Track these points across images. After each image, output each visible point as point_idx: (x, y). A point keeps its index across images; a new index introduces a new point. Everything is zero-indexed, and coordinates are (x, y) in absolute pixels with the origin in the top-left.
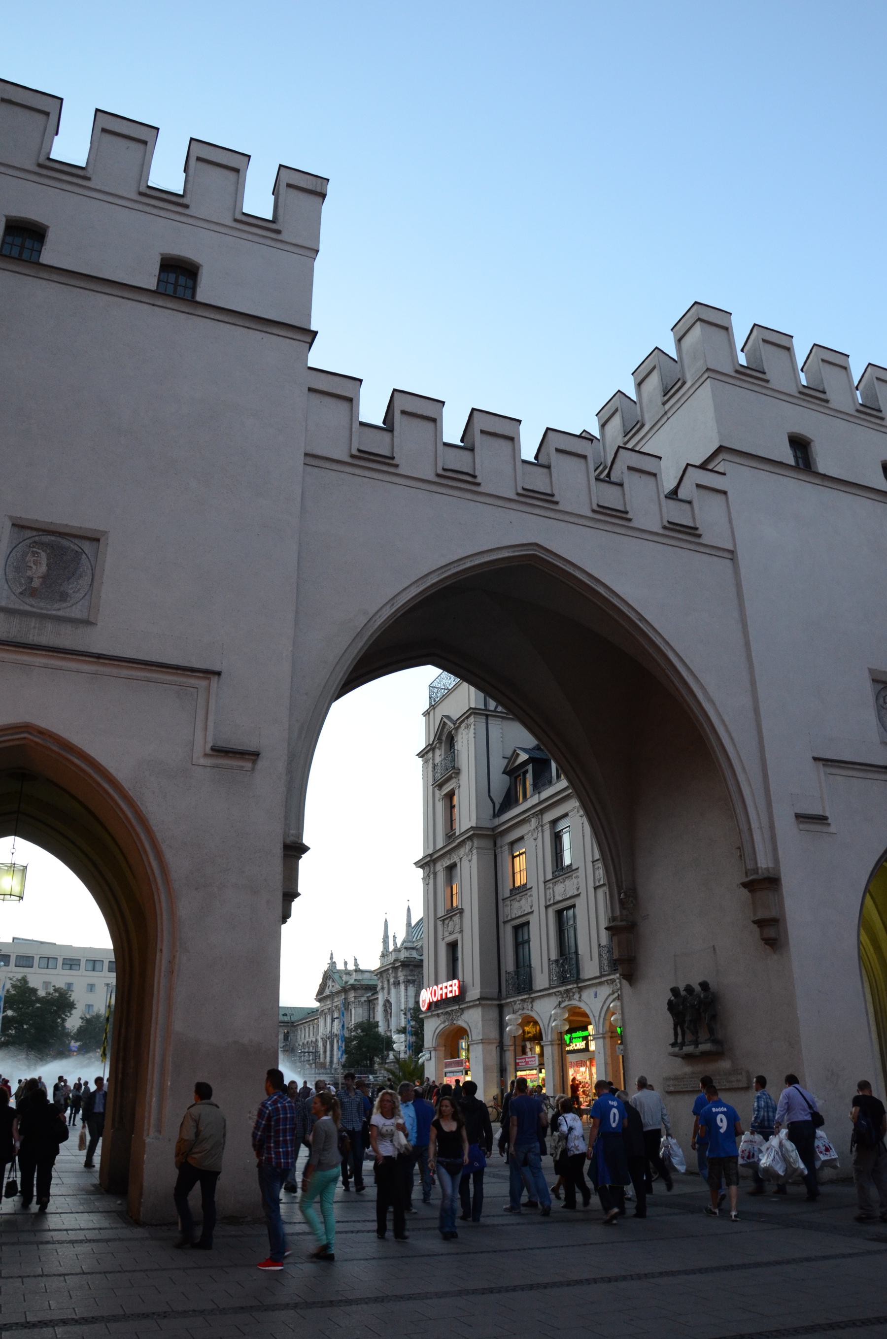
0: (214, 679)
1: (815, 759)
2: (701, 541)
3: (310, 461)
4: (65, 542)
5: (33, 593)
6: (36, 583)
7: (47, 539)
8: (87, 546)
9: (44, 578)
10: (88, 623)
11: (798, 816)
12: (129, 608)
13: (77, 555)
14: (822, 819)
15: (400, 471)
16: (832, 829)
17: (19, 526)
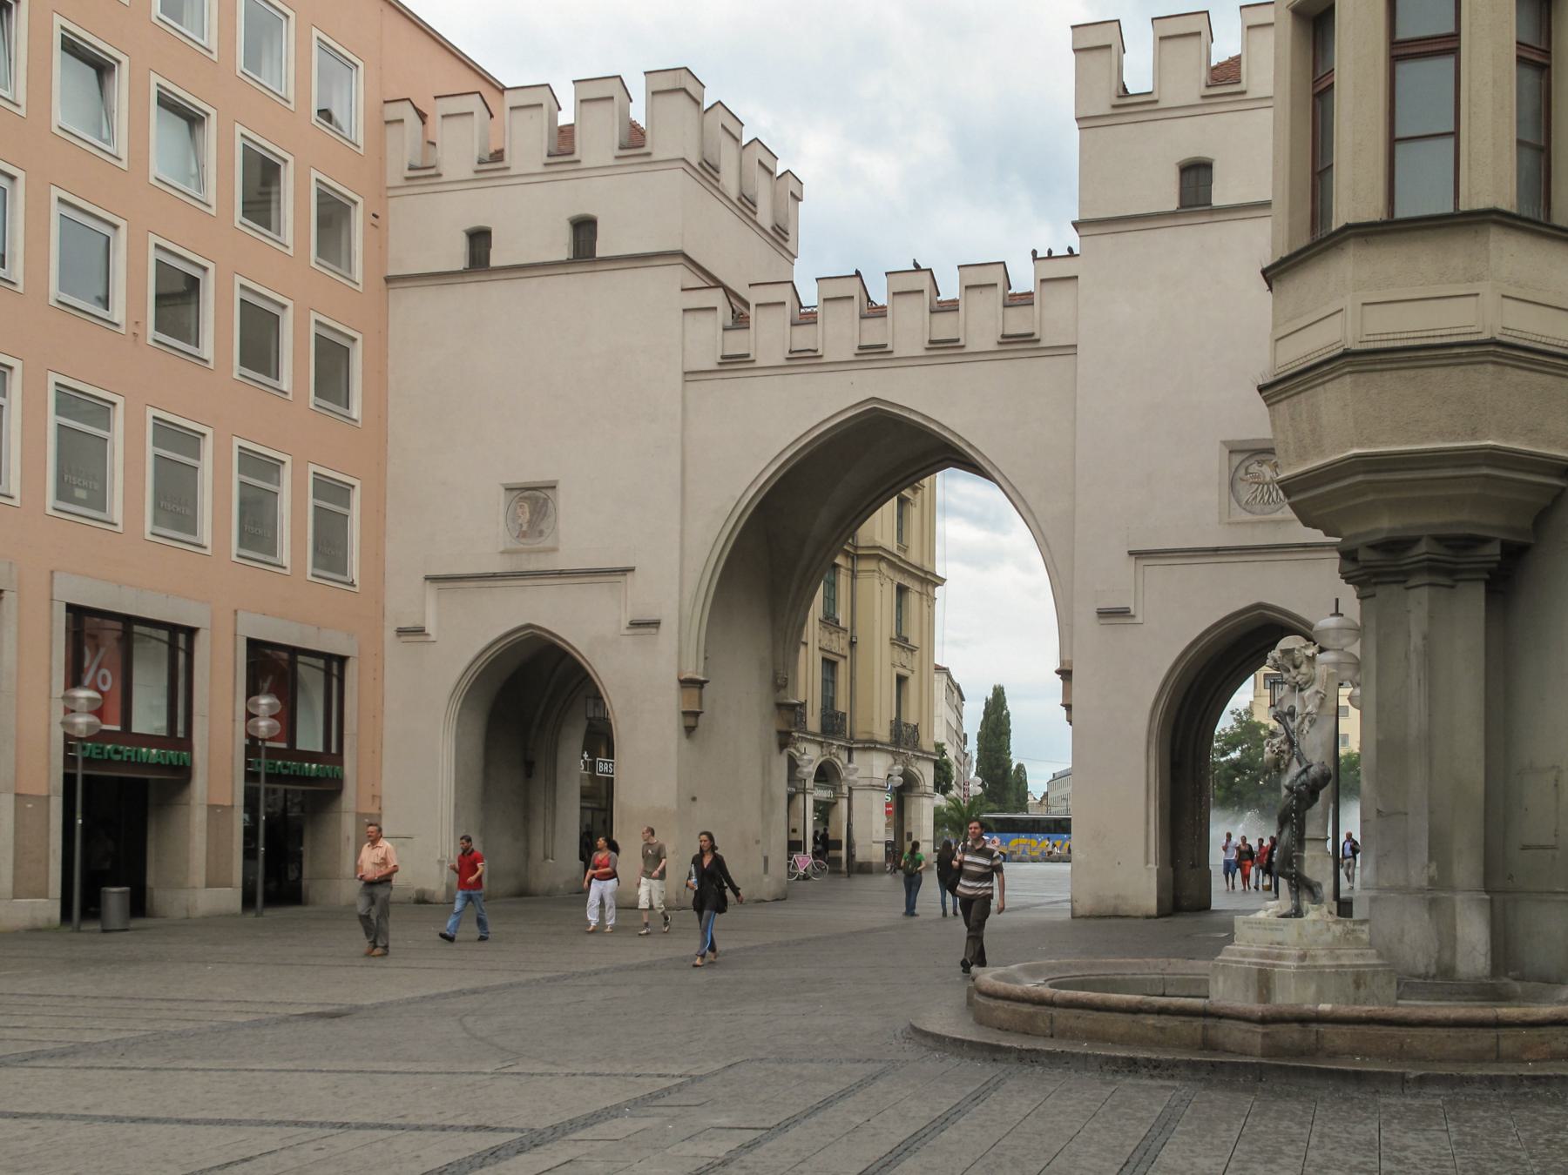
0: (629, 575)
1: (1131, 553)
2: (1041, 345)
3: (689, 377)
4: (537, 493)
5: (523, 535)
6: (525, 528)
7: (527, 494)
8: (549, 492)
9: (530, 522)
10: (554, 550)
11: (1104, 614)
12: (578, 536)
13: (546, 500)
14: (1123, 613)
15: (758, 364)
16: (1139, 619)
17: (509, 489)
